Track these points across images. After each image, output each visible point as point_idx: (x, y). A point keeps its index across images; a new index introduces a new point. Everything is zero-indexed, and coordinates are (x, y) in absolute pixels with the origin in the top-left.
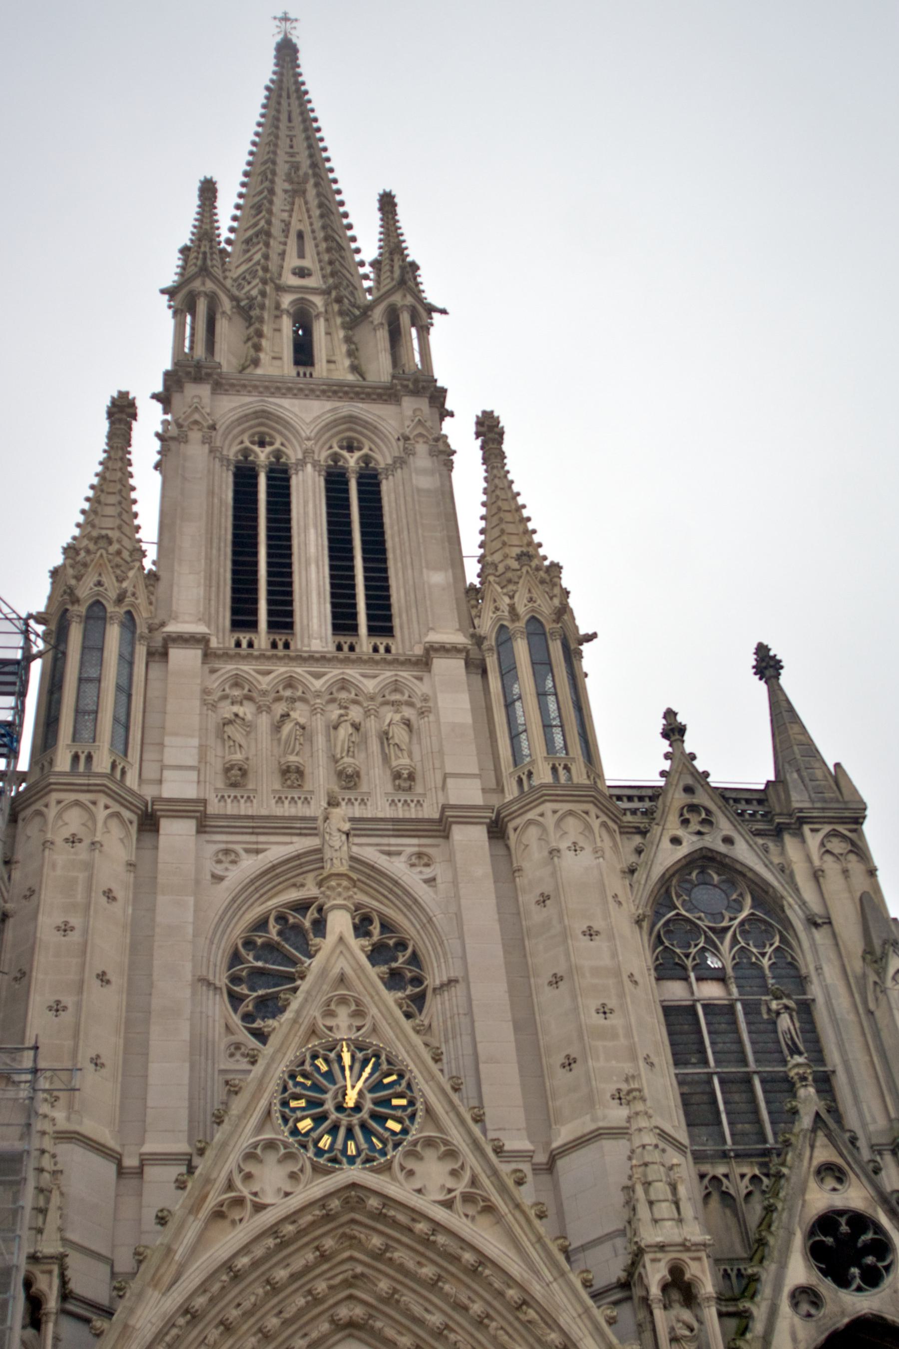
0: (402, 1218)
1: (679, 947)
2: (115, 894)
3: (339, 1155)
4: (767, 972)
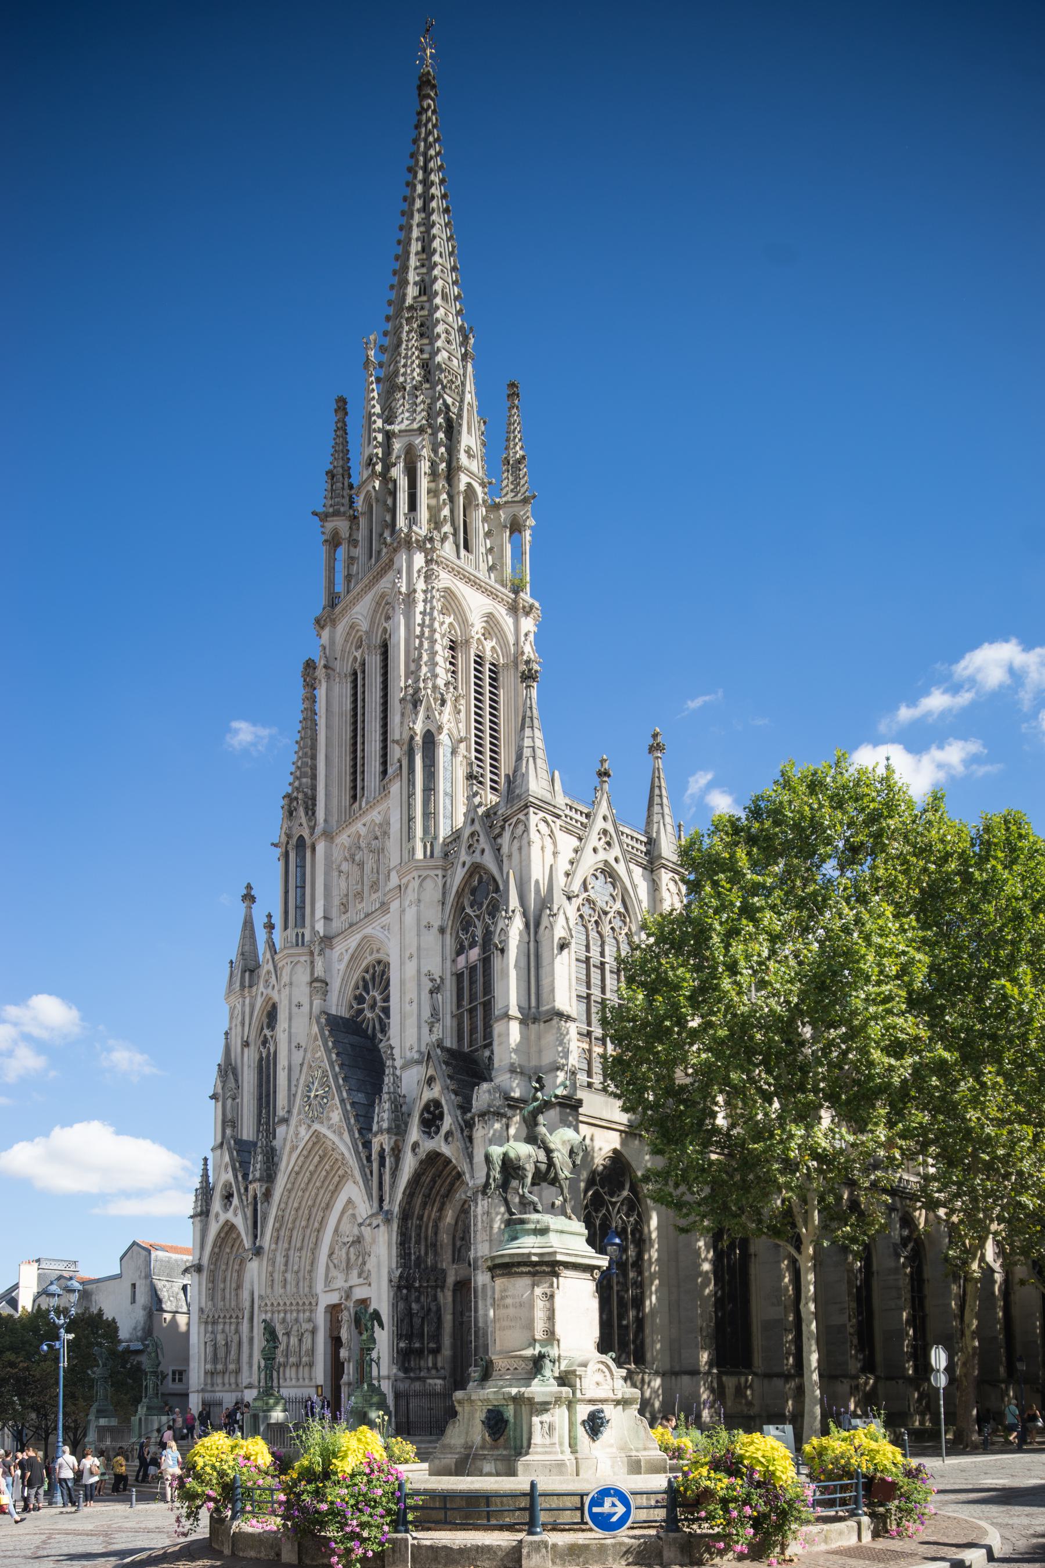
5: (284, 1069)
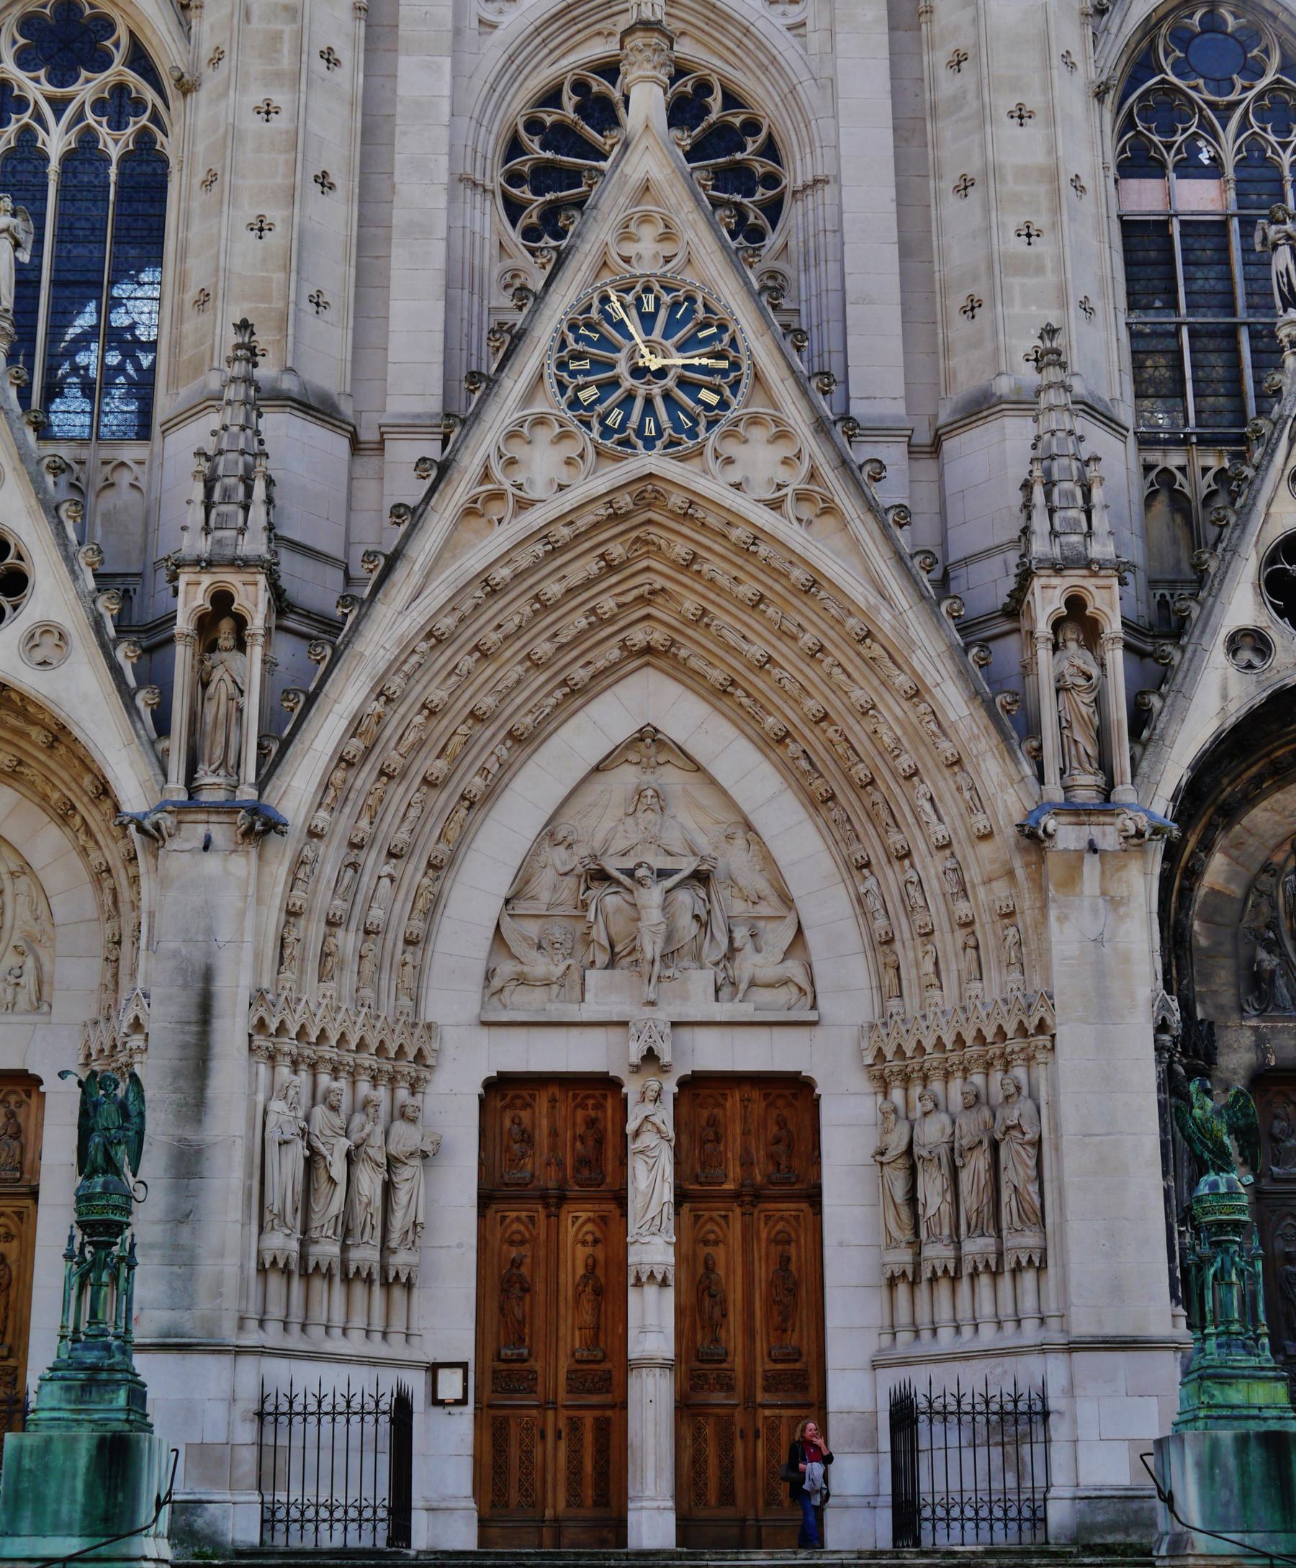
0: (711, 521)
1: (1159, 133)
2: (337, 55)
3: (633, 437)
4: (1287, 172)
5: (261, 227)
